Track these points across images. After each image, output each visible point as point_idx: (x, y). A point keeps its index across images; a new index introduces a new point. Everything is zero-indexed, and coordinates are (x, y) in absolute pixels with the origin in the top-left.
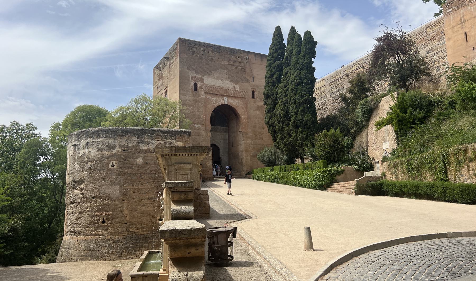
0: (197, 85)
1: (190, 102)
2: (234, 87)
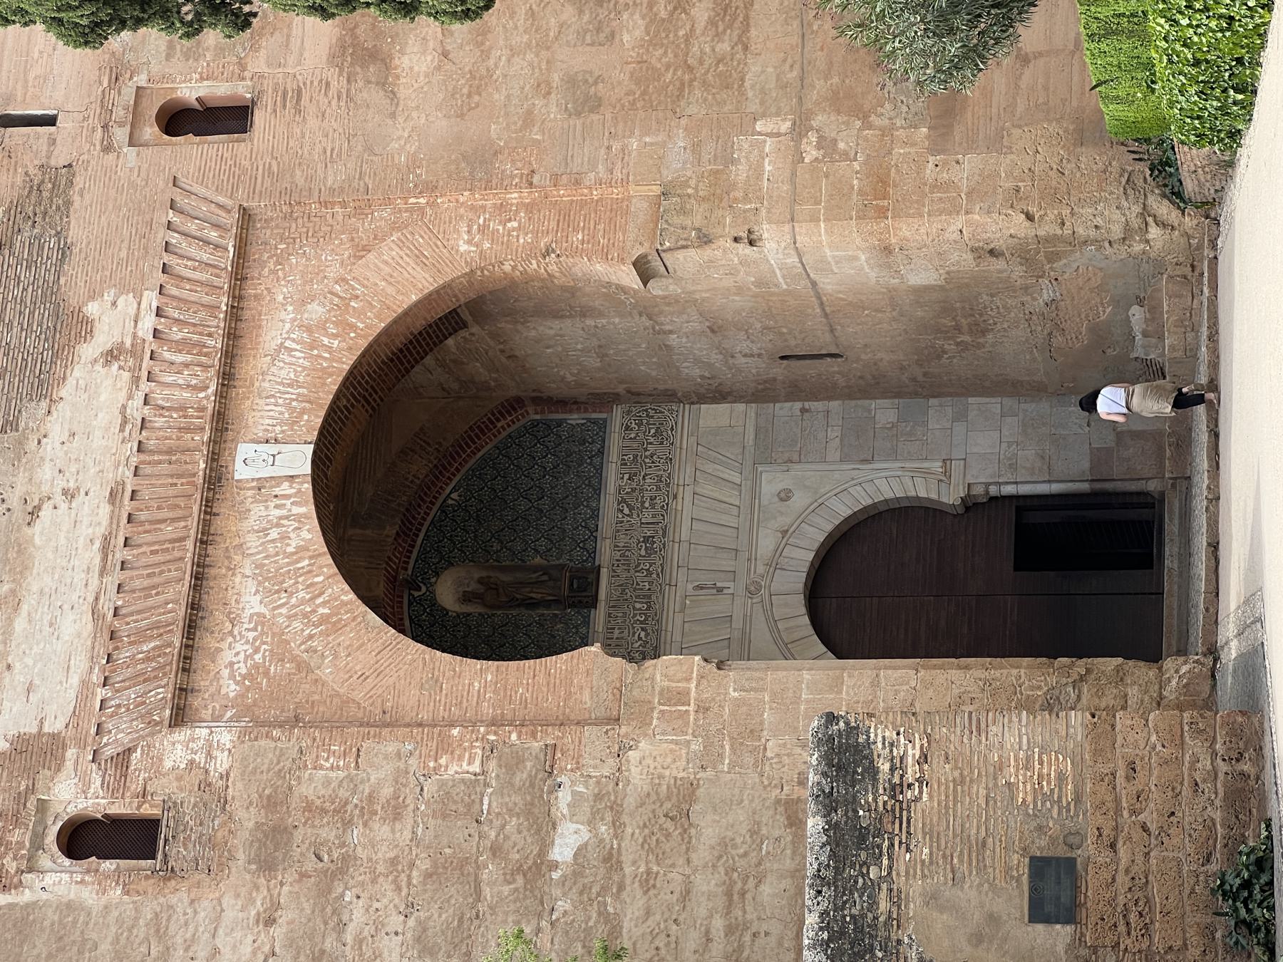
0: (97, 821)
1: (284, 917)
2: (111, 356)
